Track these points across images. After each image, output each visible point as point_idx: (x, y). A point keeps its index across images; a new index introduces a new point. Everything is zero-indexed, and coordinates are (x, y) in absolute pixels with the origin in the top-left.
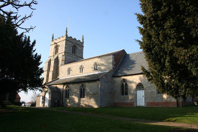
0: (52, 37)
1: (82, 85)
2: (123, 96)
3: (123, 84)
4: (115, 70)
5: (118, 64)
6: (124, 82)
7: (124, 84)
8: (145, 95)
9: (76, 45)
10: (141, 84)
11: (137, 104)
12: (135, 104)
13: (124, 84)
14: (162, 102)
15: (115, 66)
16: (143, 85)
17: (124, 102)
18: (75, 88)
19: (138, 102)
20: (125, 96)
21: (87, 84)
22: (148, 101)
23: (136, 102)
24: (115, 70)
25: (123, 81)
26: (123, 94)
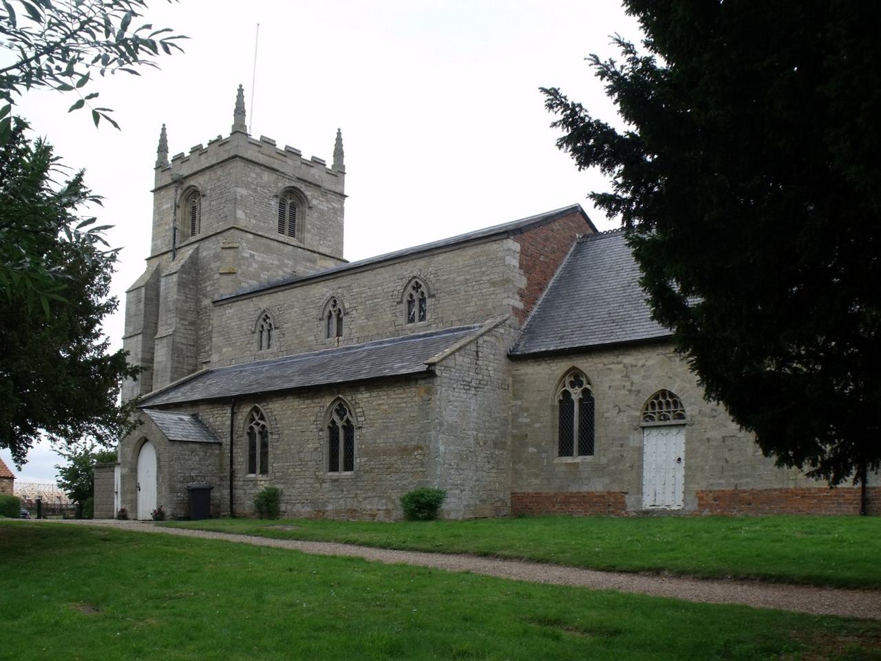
0: (119, 125)
1: (336, 406)
2: (569, 460)
3: (566, 394)
4: (521, 322)
5: (541, 290)
6: (573, 385)
7: (576, 394)
8: (690, 452)
9: (679, 404)
10: (672, 395)
11: (640, 501)
12: (630, 500)
13: (576, 394)
14: (781, 490)
15: (521, 296)
16: (682, 398)
17: (573, 489)
18: (299, 428)
19: (647, 489)
20: (579, 459)
21: (363, 397)
22: (703, 485)
23: (640, 491)
24: (521, 322)
25: (568, 380)
26: (565, 450)
